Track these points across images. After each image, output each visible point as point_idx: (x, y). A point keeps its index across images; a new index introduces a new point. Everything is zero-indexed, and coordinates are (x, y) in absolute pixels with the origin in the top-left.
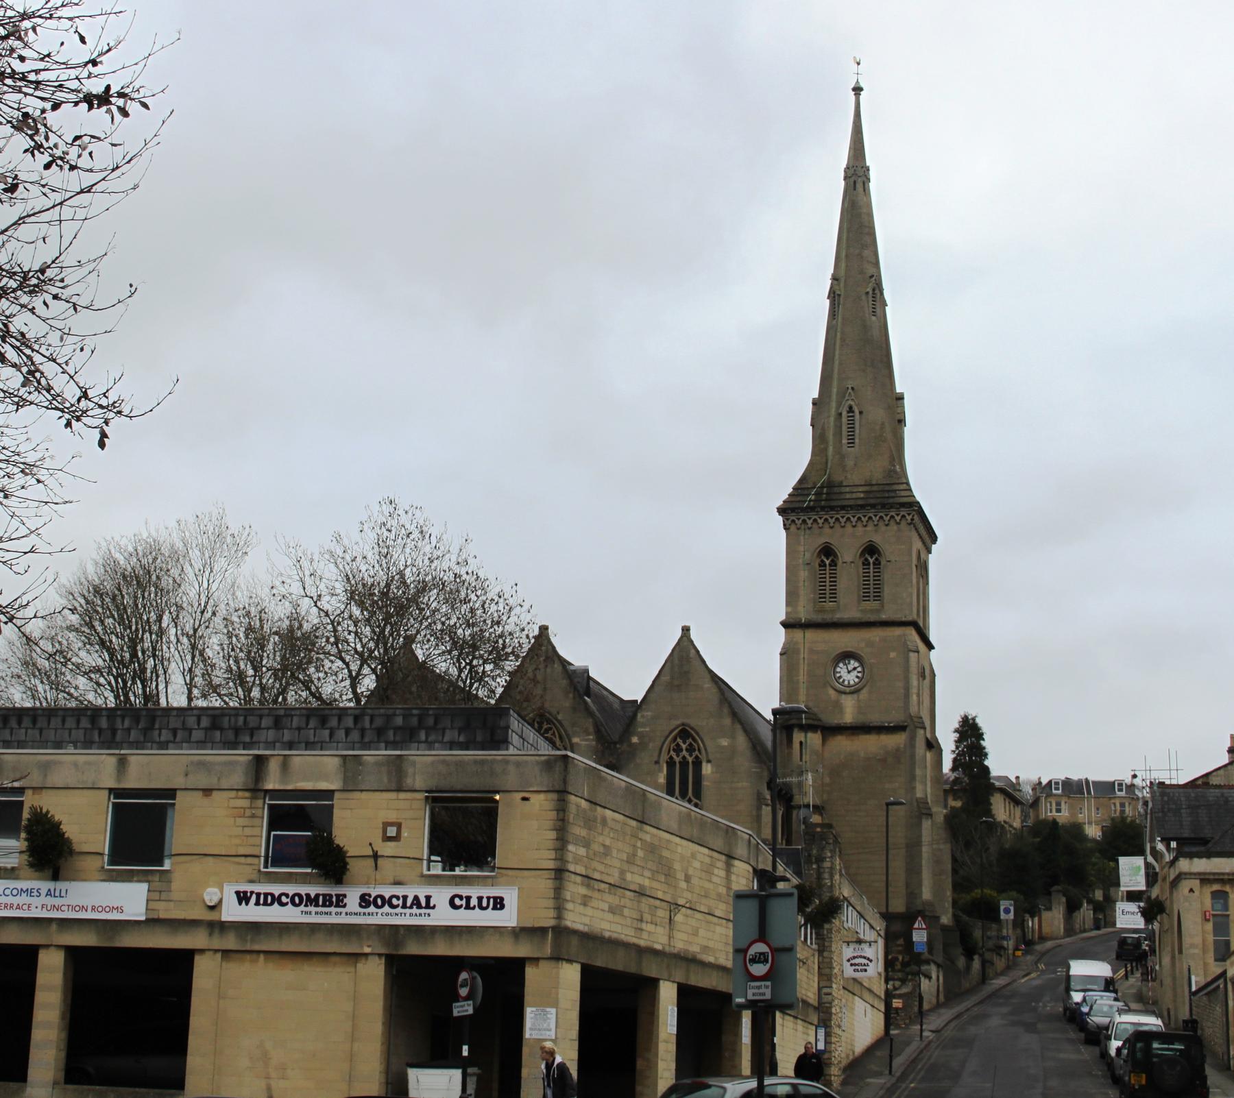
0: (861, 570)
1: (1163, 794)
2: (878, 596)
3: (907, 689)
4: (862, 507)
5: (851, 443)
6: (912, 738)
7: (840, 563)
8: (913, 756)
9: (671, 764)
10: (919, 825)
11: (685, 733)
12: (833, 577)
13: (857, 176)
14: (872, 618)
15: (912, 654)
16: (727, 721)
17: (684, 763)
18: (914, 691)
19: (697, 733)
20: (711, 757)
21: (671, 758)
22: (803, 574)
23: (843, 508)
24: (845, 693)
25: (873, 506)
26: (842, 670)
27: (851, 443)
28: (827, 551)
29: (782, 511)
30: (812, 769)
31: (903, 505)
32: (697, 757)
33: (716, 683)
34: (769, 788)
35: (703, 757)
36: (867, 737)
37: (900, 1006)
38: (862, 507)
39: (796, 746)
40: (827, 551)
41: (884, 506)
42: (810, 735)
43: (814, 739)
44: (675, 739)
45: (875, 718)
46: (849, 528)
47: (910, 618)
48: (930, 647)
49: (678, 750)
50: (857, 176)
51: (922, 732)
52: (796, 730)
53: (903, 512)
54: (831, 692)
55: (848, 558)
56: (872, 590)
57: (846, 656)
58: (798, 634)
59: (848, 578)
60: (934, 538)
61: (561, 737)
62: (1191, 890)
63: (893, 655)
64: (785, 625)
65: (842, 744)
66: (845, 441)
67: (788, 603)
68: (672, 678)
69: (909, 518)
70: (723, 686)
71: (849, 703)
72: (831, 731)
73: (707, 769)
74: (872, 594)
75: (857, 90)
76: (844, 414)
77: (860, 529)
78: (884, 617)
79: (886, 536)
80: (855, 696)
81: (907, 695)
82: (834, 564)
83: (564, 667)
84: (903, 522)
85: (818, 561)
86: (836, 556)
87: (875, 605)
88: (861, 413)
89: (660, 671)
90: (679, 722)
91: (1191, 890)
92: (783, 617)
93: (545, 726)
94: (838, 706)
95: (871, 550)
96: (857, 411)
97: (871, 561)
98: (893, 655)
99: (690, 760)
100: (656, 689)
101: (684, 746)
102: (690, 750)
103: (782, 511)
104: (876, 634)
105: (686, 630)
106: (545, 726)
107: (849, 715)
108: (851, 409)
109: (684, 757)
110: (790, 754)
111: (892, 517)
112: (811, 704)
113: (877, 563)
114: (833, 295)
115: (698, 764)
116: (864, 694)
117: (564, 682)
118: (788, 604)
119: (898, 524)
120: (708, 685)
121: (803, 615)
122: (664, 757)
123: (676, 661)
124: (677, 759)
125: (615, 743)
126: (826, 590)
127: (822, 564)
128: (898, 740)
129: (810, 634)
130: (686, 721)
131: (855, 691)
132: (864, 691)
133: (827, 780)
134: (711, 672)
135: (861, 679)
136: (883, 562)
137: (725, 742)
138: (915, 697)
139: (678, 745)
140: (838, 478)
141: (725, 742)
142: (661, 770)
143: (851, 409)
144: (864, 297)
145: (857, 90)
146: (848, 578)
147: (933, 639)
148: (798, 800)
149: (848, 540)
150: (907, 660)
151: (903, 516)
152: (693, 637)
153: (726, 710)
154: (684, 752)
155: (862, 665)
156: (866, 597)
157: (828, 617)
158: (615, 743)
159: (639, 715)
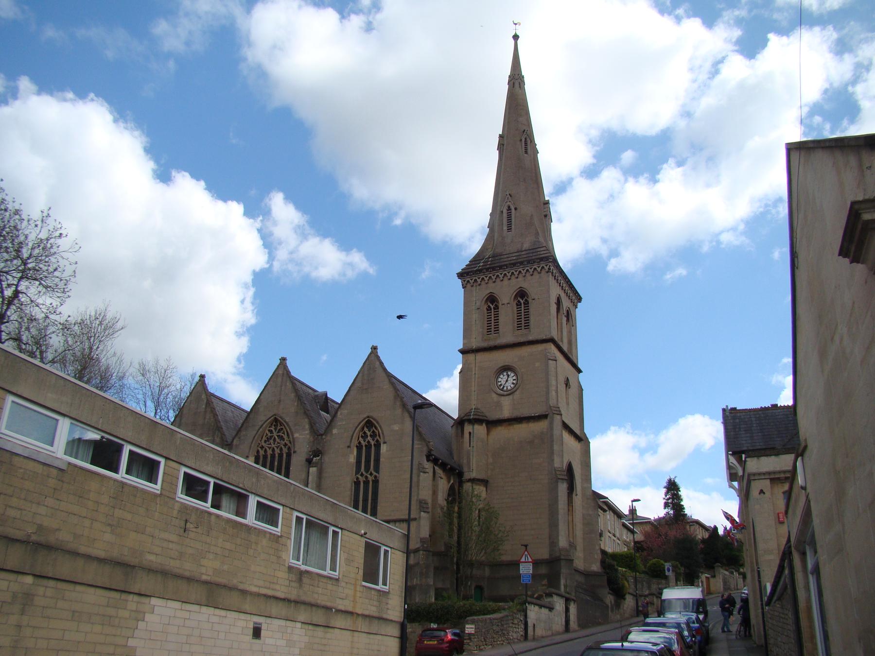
0: (515, 308)
1: (734, 418)
2: (527, 326)
3: (548, 387)
4: (514, 264)
5: (509, 229)
6: (551, 423)
7: (500, 305)
8: (552, 436)
9: (359, 447)
10: (556, 487)
11: (369, 423)
12: (497, 316)
13: (516, 80)
14: (522, 340)
15: (550, 362)
16: (399, 411)
17: (368, 446)
18: (554, 388)
19: (377, 422)
20: (387, 439)
21: (360, 443)
22: (475, 316)
23: (501, 267)
24: (503, 395)
25: (521, 263)
26: (502, 379)
27: (509, 229)
28: (492, 299)
29: (461, 275)
30: (478, 451)
31: (542, 259)
32: (377, 441)
33: (393, 384)
34: (428, 460)
35: (381, 441)
36: (520, 425)
37: (472, 631)
38: (514, 264)
39: (466, 435)
40: (492, 299)
41: (529, 262)
42: (476, 427)
43: (480, 430)
44: (363, 428)
45: (526, 412)
46: (506, 282)
47: (548, 337)
48: (579, 371)
49: (365, 436)
50: (516, 80)
51: (558, 417)
52: (466, 424)
53: (543, 264)
54: (494, 395)
55: (505, 301)
56: (523, 321)
57: (506, 369)
58: (471, 357)
59: (507, 314)
60: (580, 299)
61: (288, 435)
62: (762, 492)
63: (537, 364)
64: (463, 352)
65: (501, 432)
66: (505, 228)
67: (465, 337)
68: (363, 384)
69: (547, 268)
70: (400, 387)
71: (506, 402)
72: (492, 424)
73: (384, 448)
74: (523, 325)
75: (516, 37)
76: (505, 211)
77: (513, 280)
78: (531, 338)
79: (531, 283)
80: (511, 397)
81: (548, 393)
82: (496, 307)
83: (294, 384)
84: (543, 272)
85: (486, 306)
86: (498, 302)
87: (524, 331)
88: (516, 209)
89: (355, 380)
90: (365, 416)
91: (762, 492)
92: (461, 347)
93: (279, 428)
94: (499, 405)
95: (522, 294)
96: (513, 208)
97: (522, 302)
98: (537, 364)
99: (372, 443)
100: (352, 392)
101: (369, 433)
102: (373, 435)
103: (461, 275)
104: (525, 351)
105: (374, 348)
106: (279, 428)
107: (506, 412)
108: (509, 209)
109: (369, 442)
110: (463, 442)
111: (535, 269)
112: (479, 406)
113: (527, 303)
114: (501, 147)
115: (378, 446)
116: (517, 395)
117: (293, 395)
118: (464, 338)
119: (540, 273)
120: (386, 386)
121: (475, 345)
122: (355, 442)
123: (366, 372)
124: (363, 443)
125: (322, 435)
126: (492, 326)
127: (489, 309)
128: (540, 426)
129: (480, 356)
130: (371, 414)
131: (511, 393)
132: (518, 392)
133: (491, 460)
134: (390, 376)
135: (515, 385)
136: (530, 300)
137: (396, 427)
138: (554, 393)
139: (365, 433)
140: (499, 250)
141: (396, 427)
142: (352, 453)
143: (509, 209)
144: (519, 143)
145: (516, 37)
146: (507, 314)
147: (580, 366)
148: (467, 476)
149: (505, 290)
150: (547, 365)
151: (543, 267)
152: (379, 354)
153: (398, 403)
154: (369, 438)
155: (516, 375)
156: (519, 327)
157: (492, 343)
158: (322, 435)
159: (339, 413)
